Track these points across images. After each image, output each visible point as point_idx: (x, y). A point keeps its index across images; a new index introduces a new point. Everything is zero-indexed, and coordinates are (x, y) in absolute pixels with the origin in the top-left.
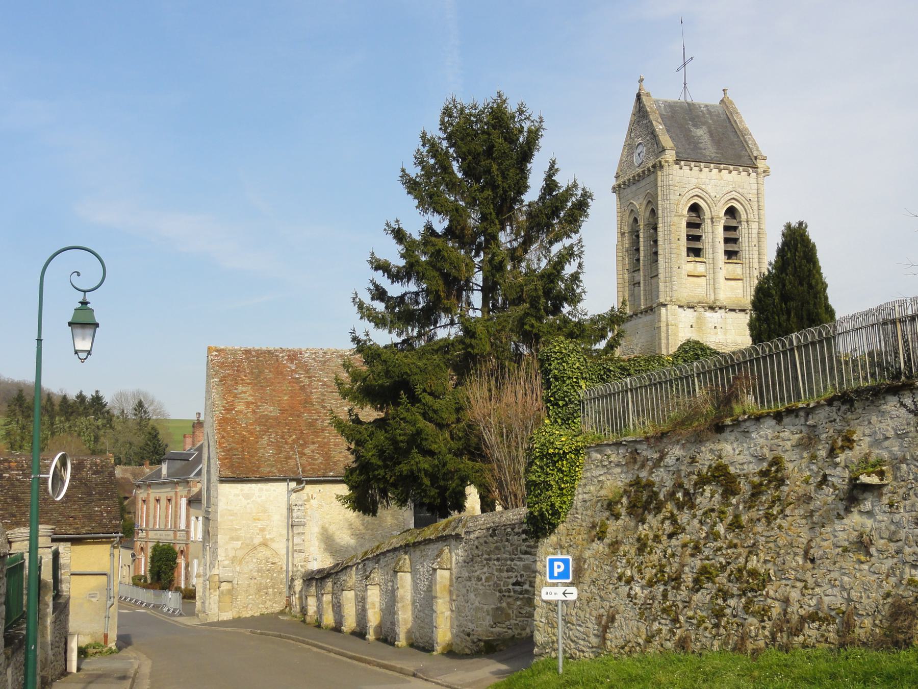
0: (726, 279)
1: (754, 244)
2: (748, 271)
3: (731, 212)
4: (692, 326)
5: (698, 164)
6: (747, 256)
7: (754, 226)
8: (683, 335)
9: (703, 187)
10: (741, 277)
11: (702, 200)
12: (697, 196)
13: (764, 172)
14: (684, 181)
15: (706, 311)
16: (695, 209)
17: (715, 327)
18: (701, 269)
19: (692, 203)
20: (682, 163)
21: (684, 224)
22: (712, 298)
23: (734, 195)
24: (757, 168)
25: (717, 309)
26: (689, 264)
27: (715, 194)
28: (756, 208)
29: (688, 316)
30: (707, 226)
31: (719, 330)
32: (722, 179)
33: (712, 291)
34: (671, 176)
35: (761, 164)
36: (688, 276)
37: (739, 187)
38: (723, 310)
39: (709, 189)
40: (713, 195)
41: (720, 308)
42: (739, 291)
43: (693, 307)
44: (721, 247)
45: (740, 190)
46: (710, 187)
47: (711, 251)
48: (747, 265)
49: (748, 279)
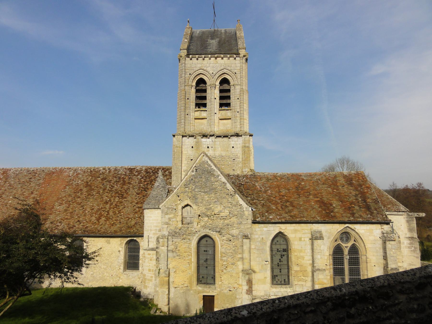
0: (220, 119)
3: (225, 81)
4: (192, 147)
5: (201, 56)
8: (186, 152)
9: (205, 68)
11: (205, 76)
12: (201, 74)
13: (244, 56)
14: (193, 66)
15: (202, 138)
16: (201, 82)
17: (208, 147)
18: (204, 114)
19: (198, 78)
20: (191, 56)
21: (193, 90)
22: (210, 130)
23: (225, 71)
24: (239, 54)
25: (208, 136)
26: (196, 112)
27: (213, 72)
28: (239, 77)
32: (217, 63)
34: (184, 64)
35: (242, 52)
36: (195, 119)
37: (228, 66)
38: (213, 137)
39: (209, 69)
40: (211, 72)
41: (211, 136)
42: (229, 126)
43: (192, 136)
44: (217, 102)
45: (229, 68)
46: (209, 68)
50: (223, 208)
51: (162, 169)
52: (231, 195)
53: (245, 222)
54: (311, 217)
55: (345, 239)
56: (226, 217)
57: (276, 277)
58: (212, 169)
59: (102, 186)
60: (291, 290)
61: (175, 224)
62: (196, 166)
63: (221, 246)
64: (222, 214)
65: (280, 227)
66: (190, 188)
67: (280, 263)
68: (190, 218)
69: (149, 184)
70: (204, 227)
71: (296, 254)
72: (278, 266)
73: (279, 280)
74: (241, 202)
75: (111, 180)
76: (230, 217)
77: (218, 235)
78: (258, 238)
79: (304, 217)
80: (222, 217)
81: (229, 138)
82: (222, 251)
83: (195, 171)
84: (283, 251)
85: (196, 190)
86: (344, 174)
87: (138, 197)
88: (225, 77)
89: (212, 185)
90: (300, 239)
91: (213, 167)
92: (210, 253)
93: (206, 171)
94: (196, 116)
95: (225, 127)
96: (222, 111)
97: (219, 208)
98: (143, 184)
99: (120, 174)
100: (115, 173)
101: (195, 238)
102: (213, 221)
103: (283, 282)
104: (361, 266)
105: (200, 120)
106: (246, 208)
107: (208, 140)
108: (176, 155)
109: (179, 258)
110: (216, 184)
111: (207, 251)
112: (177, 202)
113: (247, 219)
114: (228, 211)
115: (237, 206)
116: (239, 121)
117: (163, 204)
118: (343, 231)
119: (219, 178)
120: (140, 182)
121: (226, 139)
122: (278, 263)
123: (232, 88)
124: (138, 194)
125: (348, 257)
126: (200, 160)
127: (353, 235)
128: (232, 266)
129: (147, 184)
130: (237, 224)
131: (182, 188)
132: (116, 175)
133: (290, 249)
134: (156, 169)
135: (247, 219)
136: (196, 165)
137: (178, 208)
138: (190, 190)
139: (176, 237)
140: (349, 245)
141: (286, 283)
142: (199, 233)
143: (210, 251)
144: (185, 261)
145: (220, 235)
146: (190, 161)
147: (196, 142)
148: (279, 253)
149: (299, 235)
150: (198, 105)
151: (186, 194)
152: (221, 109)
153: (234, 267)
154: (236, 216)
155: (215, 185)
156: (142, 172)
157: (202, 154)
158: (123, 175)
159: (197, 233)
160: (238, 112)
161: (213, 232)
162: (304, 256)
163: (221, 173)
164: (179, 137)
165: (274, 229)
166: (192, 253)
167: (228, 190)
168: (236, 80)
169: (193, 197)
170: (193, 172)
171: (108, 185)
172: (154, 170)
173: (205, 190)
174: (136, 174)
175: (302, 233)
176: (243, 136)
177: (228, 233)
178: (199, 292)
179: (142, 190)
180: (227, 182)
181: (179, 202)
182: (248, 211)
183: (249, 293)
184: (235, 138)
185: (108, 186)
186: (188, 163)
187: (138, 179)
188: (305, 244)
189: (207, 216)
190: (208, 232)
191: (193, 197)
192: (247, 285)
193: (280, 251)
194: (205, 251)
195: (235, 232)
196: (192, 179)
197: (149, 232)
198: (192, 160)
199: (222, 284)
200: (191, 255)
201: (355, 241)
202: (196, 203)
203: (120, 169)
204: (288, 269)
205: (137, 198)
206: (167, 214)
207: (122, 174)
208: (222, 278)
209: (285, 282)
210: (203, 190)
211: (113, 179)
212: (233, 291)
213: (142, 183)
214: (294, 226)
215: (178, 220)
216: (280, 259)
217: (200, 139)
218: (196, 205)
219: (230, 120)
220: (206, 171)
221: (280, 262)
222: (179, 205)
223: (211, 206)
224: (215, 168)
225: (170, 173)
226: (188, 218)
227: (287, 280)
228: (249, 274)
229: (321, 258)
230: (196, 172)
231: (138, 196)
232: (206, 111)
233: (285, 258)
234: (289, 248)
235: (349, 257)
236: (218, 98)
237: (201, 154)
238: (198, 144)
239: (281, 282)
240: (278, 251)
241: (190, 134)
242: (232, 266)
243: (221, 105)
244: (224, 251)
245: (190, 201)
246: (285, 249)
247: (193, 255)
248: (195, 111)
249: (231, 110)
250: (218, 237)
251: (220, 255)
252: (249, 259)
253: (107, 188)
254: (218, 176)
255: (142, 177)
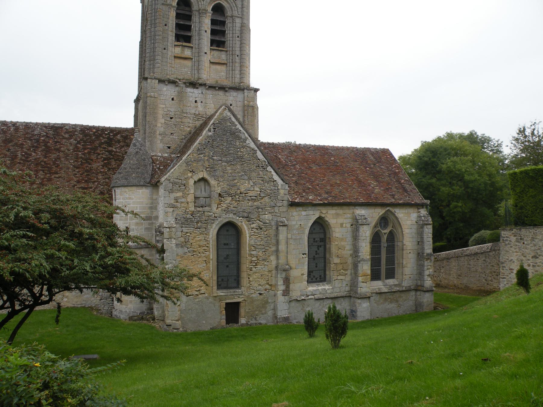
1: (237, 35)
2: (231, 58)
3: (218, 9)
6: (231, 45)
7: (238, 21)
10: (226, 62)
15: (187, 87)
17: (196, 102)
18: (188, 53)
21: (173, 14)
22: (196, 76)
28: (240, 6)
29: (169, 91)
30: (195, 18)
31: (199, 104)
33: (196, 71)
41: (201, 85)
42: (223, 74)
47: (197, 38)
48: (231, 52)
49: (231, 64)
50: (252, 184)
51: (109, 131)
52: (262, 167)
53: (281, 204)
54: (354, 198)
55: (383, 226)
56: (256, 197)
57: (311, 273)
58: (238, 129)
59: (8, 153)
60: (329, 286)
61: (184, 207)
62: (214, 124)
63: (250, 237)
64: (251, 194)
65: (320, 210)
66: (207, 154)
67: (316, 256)
68: (205, 199)
69: (92, 154)
70: (227, 211)
71: (336, 243)
72: (314, 259)
73: (314, 277)
74: (276, 177)
75: (22, 144)
76: (261, 198)
77: (245, 222)
78: (294, 225)
79: (346, 198)
80: (250, 196)
81: (226, 91)
82: (251, 243)
83: (212, 130)
84: (321, 241)
85: (215, 158)
86: (371, 151)
87: (77, 172)
88: (220, 1)
89: (238, 152)
90: (342, 225)
91: (239, 126)
92: (232, 247)
93: (228, 132)
94: (177, 53)
95: (218, 75)
96: (215, 51)
97: (246, 185)
98: (82, 153)
99: (38, 135)
100: (27, 133)
101: (214, 226)
102: (238, 202)
103: (318, 279)
104: (396, 255)
105: (182, 61)
106: (282, 185)
107: (196, 91)
108: (150, 108)
109: (192, 254)
110: (242, 150)
111: (227, 244)
112: (187, 174)
113: (283, 201)
114: (258, 190)
115: (270, 183)
116: (238, 68)
117: (166, 177)
118: (383, 216)
119: (247, 142)
120: (76, 149)
121: (221, 93)
122: (314, 256)
123: (228, 21)
124: (77, 168)
125: (386, 245)
126: (221, 114)
127: (392, 220)
128: (263, 262)
129: (89, 153)
130: (270, 207)
131: (194, 154)
132: (30, 135)
133: (330, 238)
134: (99, 131)
135: (283, 201)
136: (214, 121)
137: (188, 183)
138: (206, 158)
139: (187, 226)
140: (387, 231)
141: (322, 280)
142: (220, 219)
143: (233, 244)
144: (200, 259)
145: (248, 221)
146: (169, 119)
147: (178, 92)
148: (316, 244)
149: (340, 220)
150: (178, 38)
151: (200, 163)
152: (211, 48)
153: (265, 263)
154: (269, 196)
155: (241, 152)
156: (76, 133)
157: (223, 107)
158: (43, 136)
159: (217, 220)
160: (238, 56)
161: (239, 217)
162: (345, 246)
163: (249, 136)
164: (153, 81)
165: (313, 215)
166: (210, 248)
167: (259, 159)
168: (236, 9)
169: (211, 168)
170: (210, 131)
171: (18, 151)
172: (95, 132)
173: (228, 159)
174: (67, 136)
175: (344, 217)
176: (245, 91)
177: (259, 219)
178: (220, 299)
179: (81, 162)
180: (256, 149)
181: (190, 175)
182: (284, 189)
183: (285, 294)
184: (234, 93)
185: (19, 154)
186: (166, 122)
187: (71, 144)
188: (346, 231)
189: (230, 195)
190: (233, 218)
191: (211, 168)
192: (284, 285)
193: (317, 241)
194: (225, 244)
195: (267, 217)
196: (209, 142)
197: (129, 221)
198: (171, 118)
199: (251, 286)
200: (209, 250)
201: (392, 227)
202: (216, 178)
203: (36, 127)
204: (325, 262)
205: (76, 174)
206: (171, 191)
207: (40, 135)
208: (251, 279)
209: (320, 279)
210: (225, 159)
211: (26, 142)
212: (264, 294)
213: (80, 151)
214: (336, 210)
215: (189, 200)
216: (316, 252)
217: (184, 88)
218: (215, 179)
219: (225, 66)
220: (228, 132)
221: (316, 254)
222: (191, 179)
223: (236, 181)
224: (241, 129)
225: (124, 138)
226: (201, 198)
227: (322, 276)
228: (286, 271)
229: (366, 246)
230: (214, 131)
231: (78, 170)
232: (192, 47)
233: (322, 249)
234: (328, 236)
235: (387, 245)
236: (209, 32)
237: (221, 107)
238: (181, 96)
239: (316, 279)
240: (314, 242)
241: (172, 78)
242: (263, 262)
243: (213, 42)
244: (253, 243)
245: (207, 173)
246: (323, 239)
247: (211, 250)
248: (175, 45)
249: (227, 51)
250: (246, 224)
251: (248, 249)
252: (285, 251)
253: (18, 155)
254: (246, 139)
255: (78, 141)
